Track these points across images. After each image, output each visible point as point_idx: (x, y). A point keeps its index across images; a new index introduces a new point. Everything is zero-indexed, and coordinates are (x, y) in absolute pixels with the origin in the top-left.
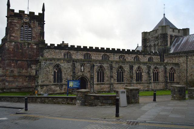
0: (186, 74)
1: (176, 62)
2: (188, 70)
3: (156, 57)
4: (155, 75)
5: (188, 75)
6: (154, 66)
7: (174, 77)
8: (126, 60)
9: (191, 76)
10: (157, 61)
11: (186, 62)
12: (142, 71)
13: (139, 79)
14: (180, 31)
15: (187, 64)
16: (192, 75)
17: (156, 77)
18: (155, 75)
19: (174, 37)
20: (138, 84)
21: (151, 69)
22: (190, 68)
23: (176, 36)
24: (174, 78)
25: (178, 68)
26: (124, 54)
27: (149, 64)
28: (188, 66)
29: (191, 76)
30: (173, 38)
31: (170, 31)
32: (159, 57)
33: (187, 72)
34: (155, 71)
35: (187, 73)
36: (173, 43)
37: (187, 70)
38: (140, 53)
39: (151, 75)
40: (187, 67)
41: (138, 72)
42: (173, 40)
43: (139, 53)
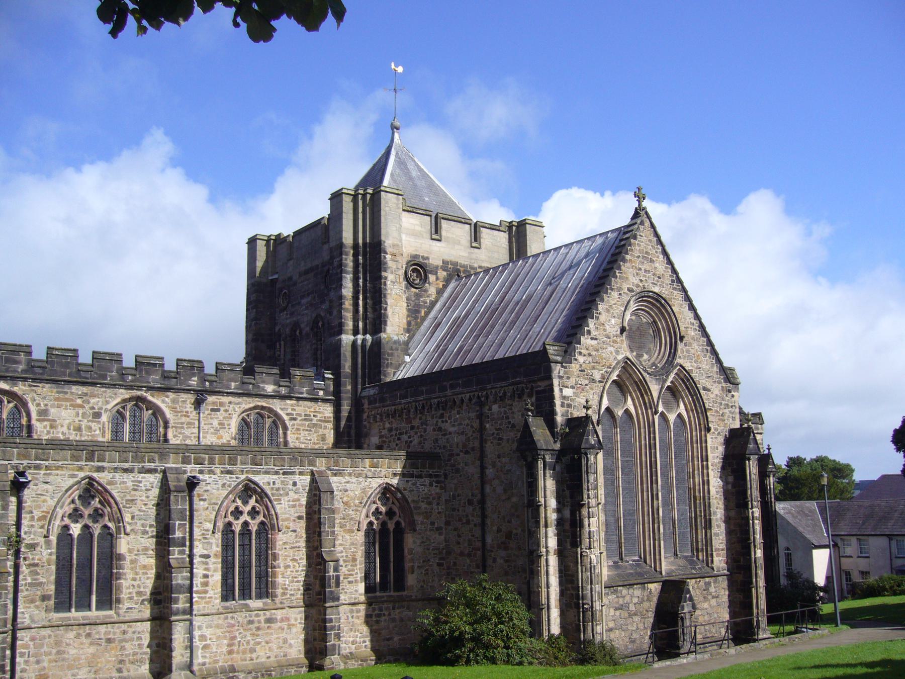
0: (478, 532)
1: (428, 446)
2: (488, 504)
3: (304, 408)
4: (245, 547)
5: (489, 540)
6: (232, 481)
7: (407, 557)
8: (30, 427)
9: (504, 546)
10: (314, 437)
11: (477, 444)
12: (121, 519)
13: (90, 593)
14: (485, 233)
15: (482, 457)
16: (509, 535)
17: (245, 566)
18: (245, 547)
19: (442, 274)
20: (71, 634)
21: (199, 505)
22: (499, 490)
23: (455, 272)
24: (408, 565)
25: (435, 490)
26: (14, 379)
27: (186, 461)
28: (490, 472)
29: (504, 546)
30: (432, 278)
31: (414, 234)
32: (328, 411)
33: (484, 516)
34: (245, 517)
35: (483, 525)
36: (433, 314)
37: (482, 502)
38: (166, 376)
39: (198, 550)
40: (483, 483)
41: (76, 530)
42: (432, 291)
43: (155, 379)
